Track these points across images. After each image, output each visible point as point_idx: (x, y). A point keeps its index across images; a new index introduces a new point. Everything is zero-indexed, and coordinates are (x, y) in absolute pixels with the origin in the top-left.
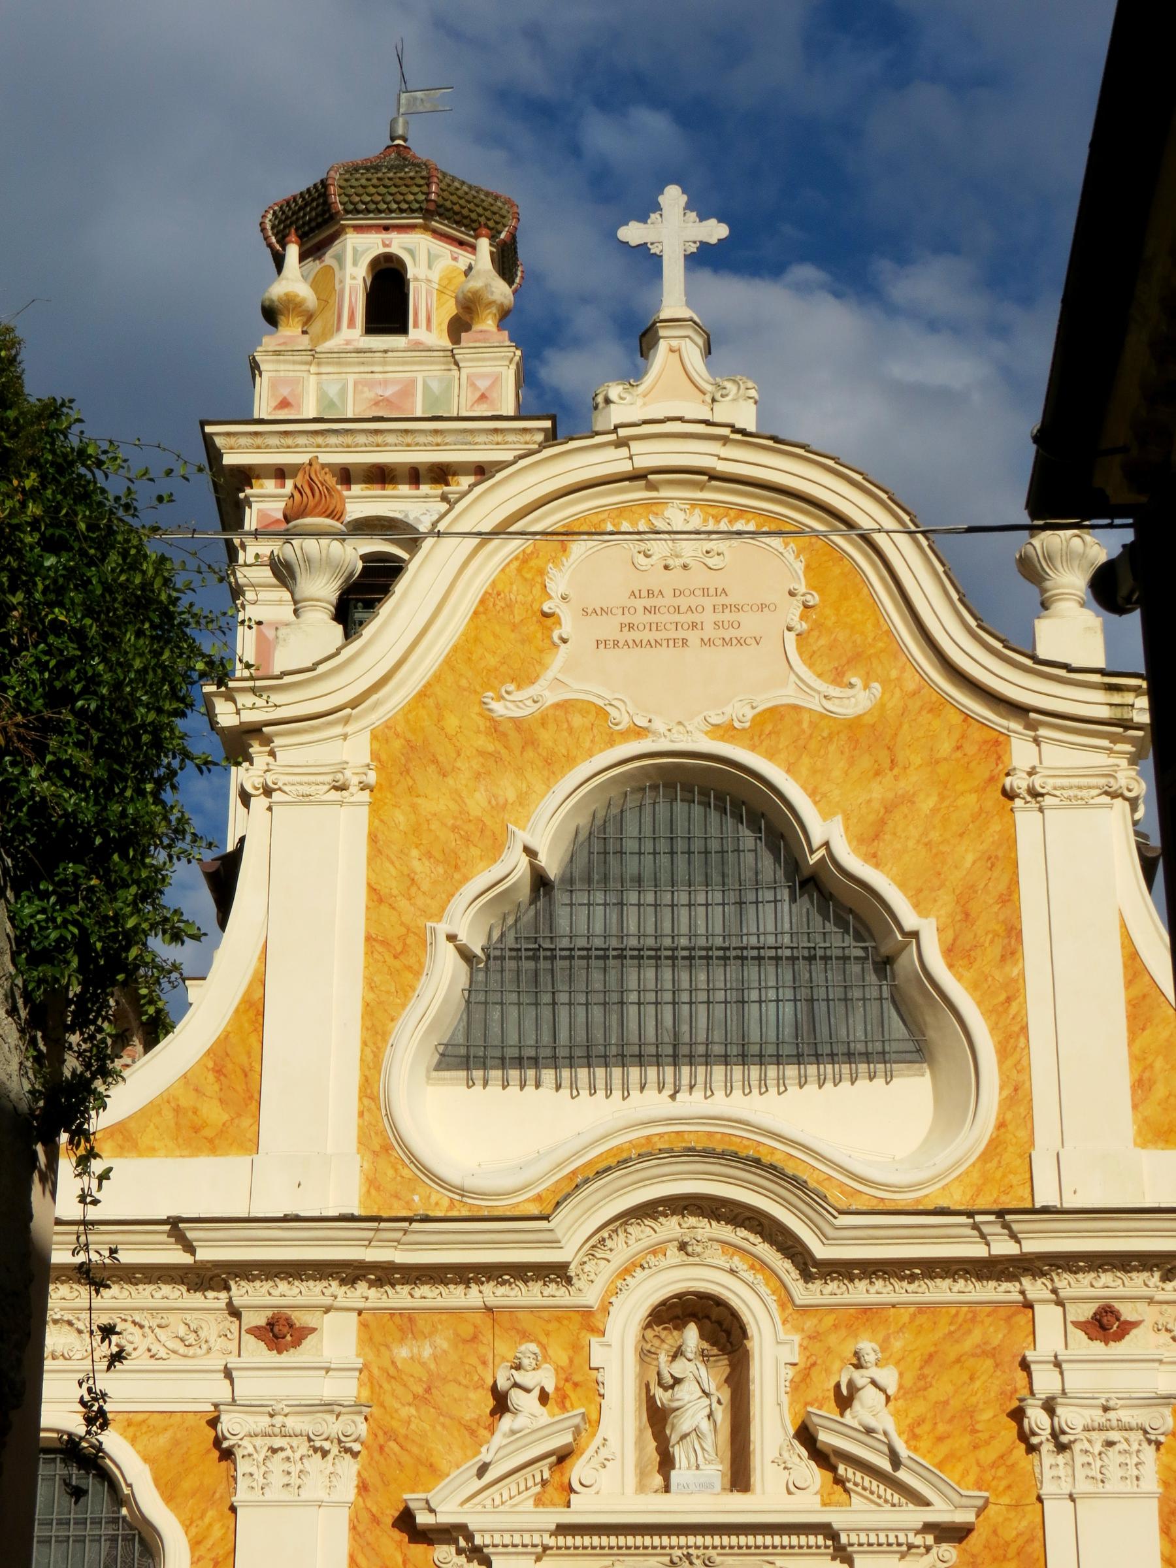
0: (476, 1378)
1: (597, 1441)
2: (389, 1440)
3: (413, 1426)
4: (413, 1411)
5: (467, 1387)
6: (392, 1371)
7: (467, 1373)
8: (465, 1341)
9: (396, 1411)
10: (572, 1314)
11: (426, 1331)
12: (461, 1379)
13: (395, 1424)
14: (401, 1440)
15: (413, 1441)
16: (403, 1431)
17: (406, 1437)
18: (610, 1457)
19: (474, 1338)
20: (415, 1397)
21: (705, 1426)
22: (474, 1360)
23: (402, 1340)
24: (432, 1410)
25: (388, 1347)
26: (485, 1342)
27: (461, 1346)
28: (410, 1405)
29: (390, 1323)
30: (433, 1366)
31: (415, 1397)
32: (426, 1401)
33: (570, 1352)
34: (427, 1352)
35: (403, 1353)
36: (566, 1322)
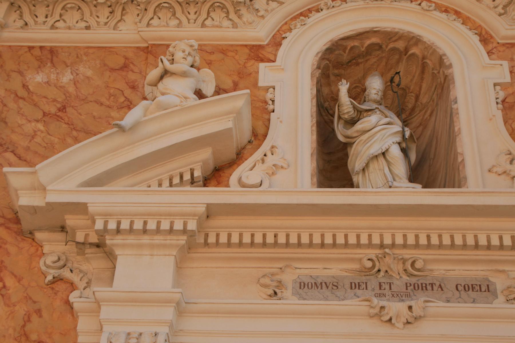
0: (122, 99)
1: (266, 146)
2: (6, 151)
3: (38, 140)
4: (40, 126)
5: (109, 107)
6: (22, 93)
7: (111, 95)
8: (112, 70)
9: (20, 126)
10: (238, 48)
11: (69, 62)
12: (103, 100)
13: (14, 137)
14: (20, 151)
15: (36, 153)
16: (24, 143)
17: (28, 149)
18: (280, 164)
19: (125, 67)
20: (45, 114)
21: (395, 152)
22: (121, 85)
23: (39, 68)
24: (64, 126)
25: (20, 73)
26: (136, 70)
27: (108, 73)
28: (37, 121)
29: (29, 54)
30: (71, 89)
31: (45, 114)
32: (58, 118)
33: (236, 78)
34: (67, 78)
35: (39, 78)
36: (231, 54)
